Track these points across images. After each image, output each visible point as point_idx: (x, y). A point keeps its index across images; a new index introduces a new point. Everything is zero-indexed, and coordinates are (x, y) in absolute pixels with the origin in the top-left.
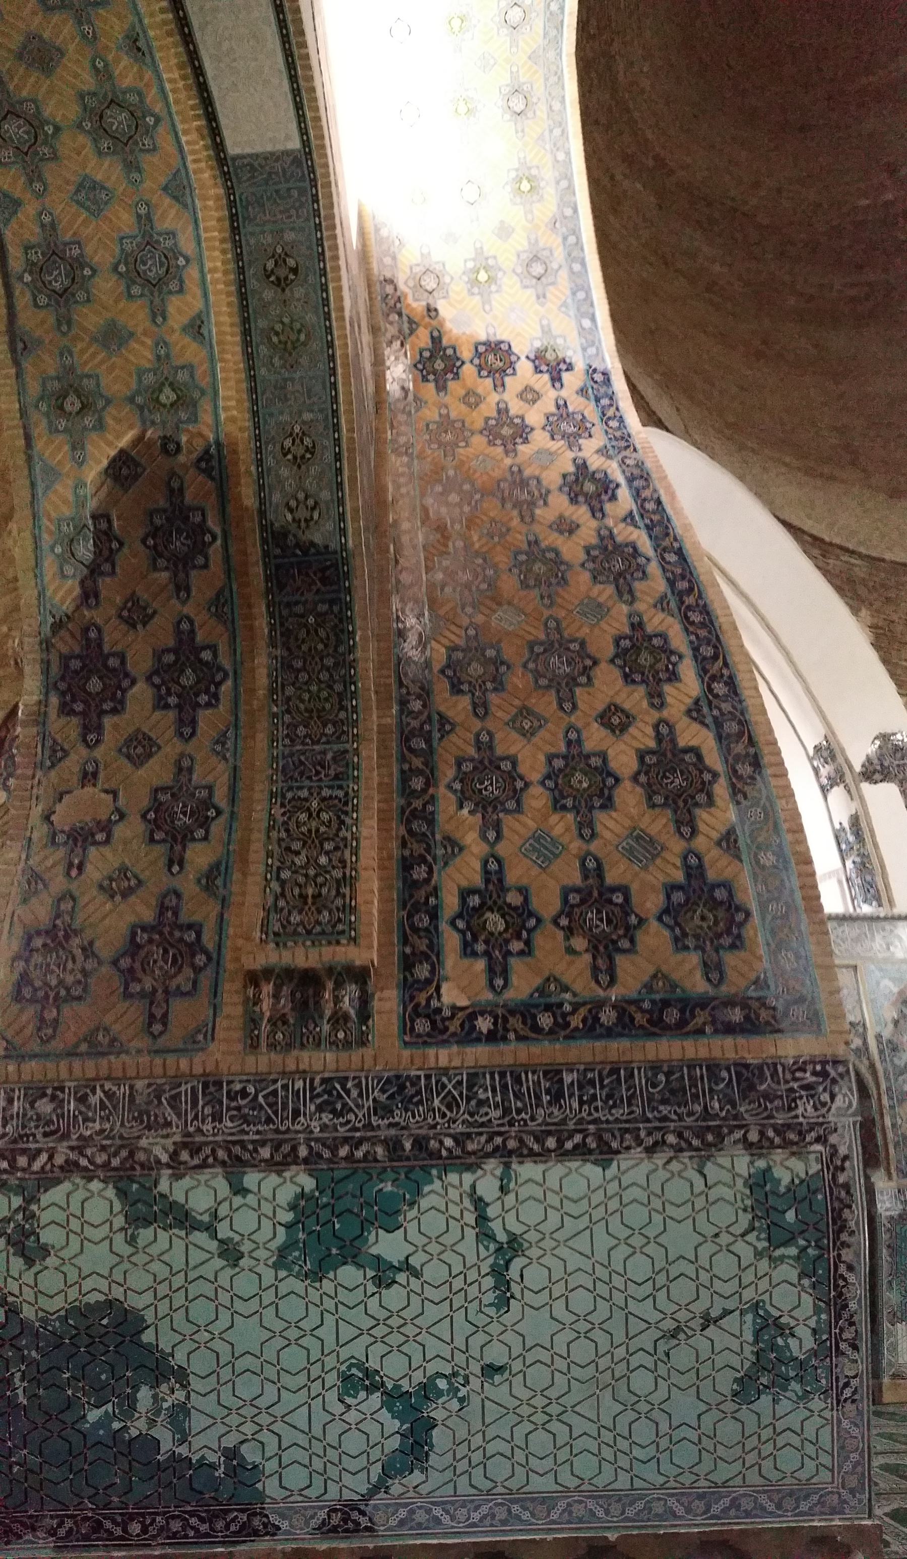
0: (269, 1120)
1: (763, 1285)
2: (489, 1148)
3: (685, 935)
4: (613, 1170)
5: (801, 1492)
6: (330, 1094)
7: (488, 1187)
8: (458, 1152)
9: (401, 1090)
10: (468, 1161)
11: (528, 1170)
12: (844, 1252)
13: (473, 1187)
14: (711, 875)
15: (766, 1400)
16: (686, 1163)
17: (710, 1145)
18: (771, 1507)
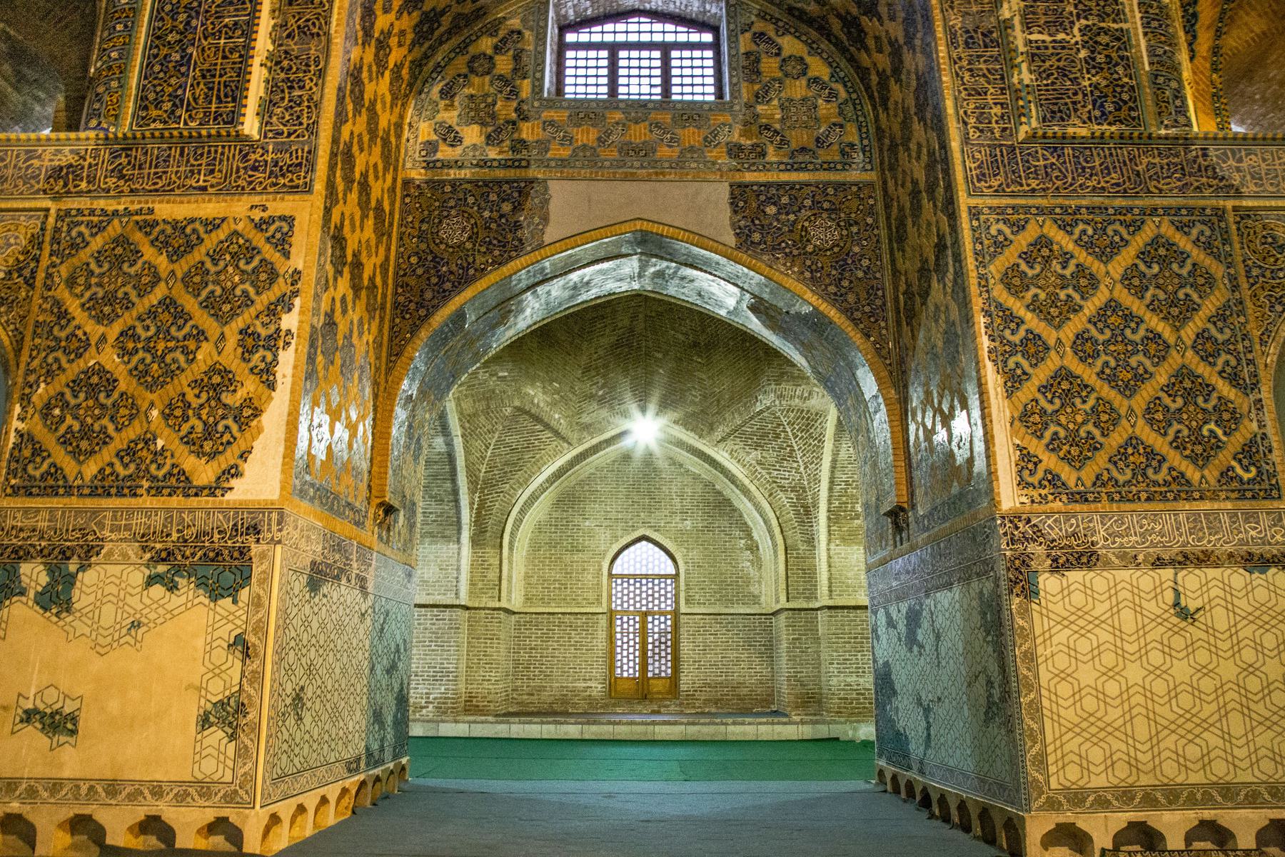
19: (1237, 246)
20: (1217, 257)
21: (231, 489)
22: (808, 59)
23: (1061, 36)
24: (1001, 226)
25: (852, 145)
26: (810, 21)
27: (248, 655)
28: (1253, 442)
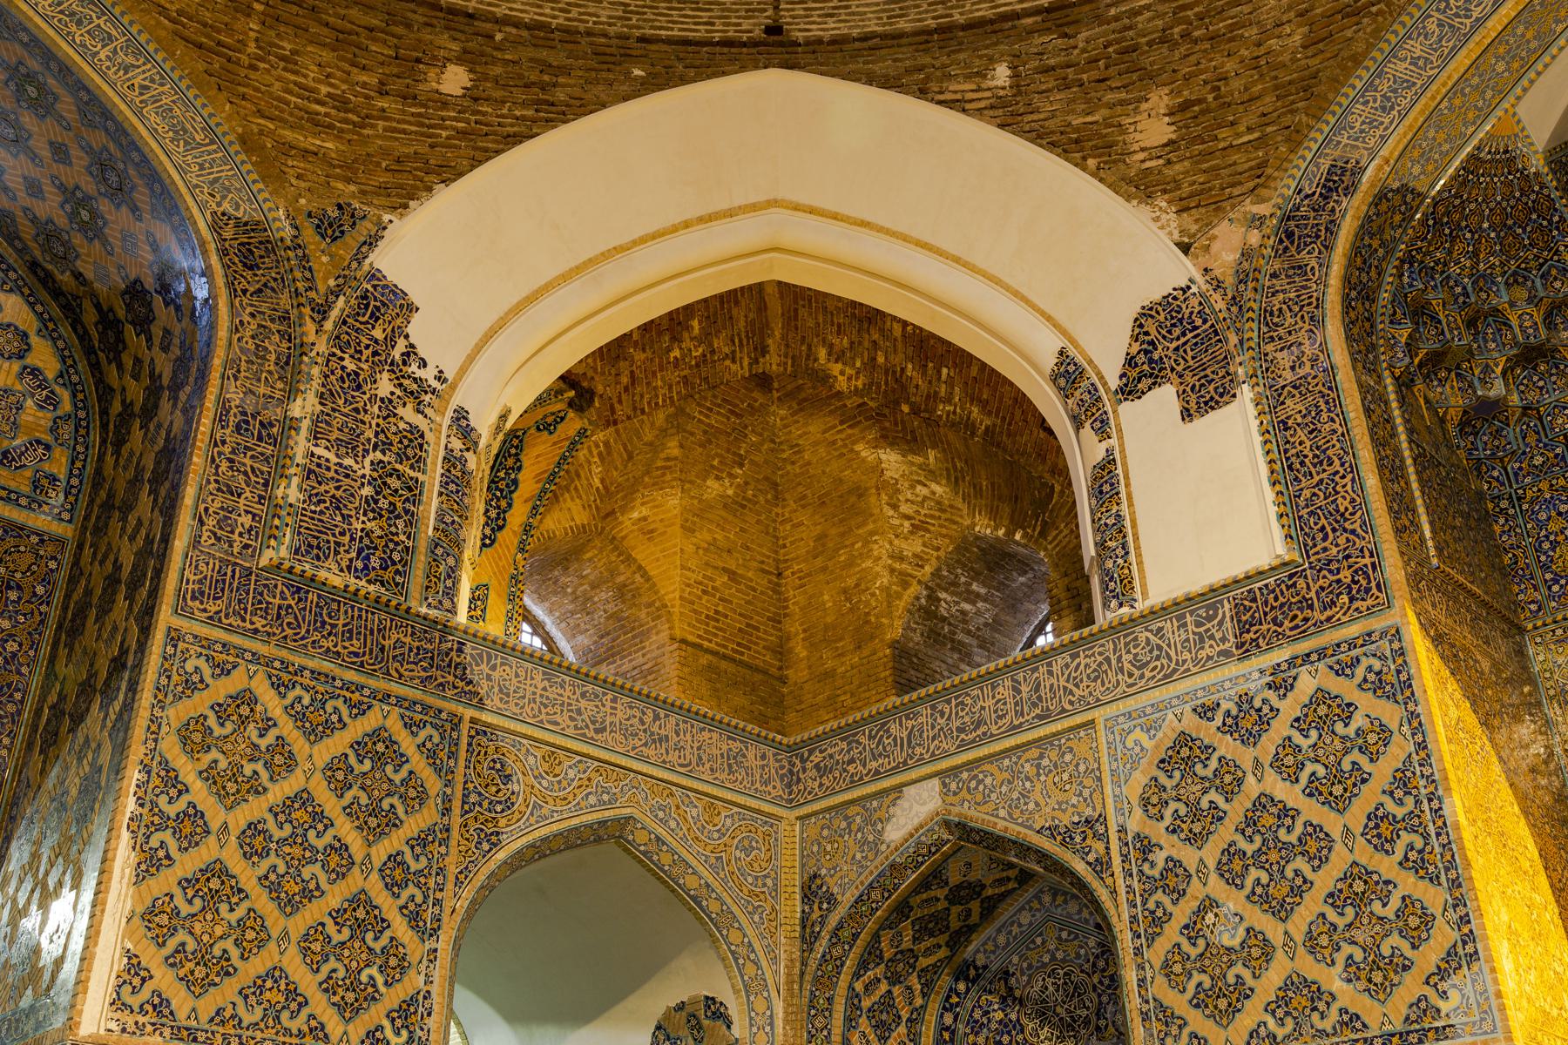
19: (462, 763)
20: (438, 771)
22: (34, 339)
23: (349, 462)
24: (202, 663)
25: (53, 479)
26: (57, 293)
28: (413, 1000)
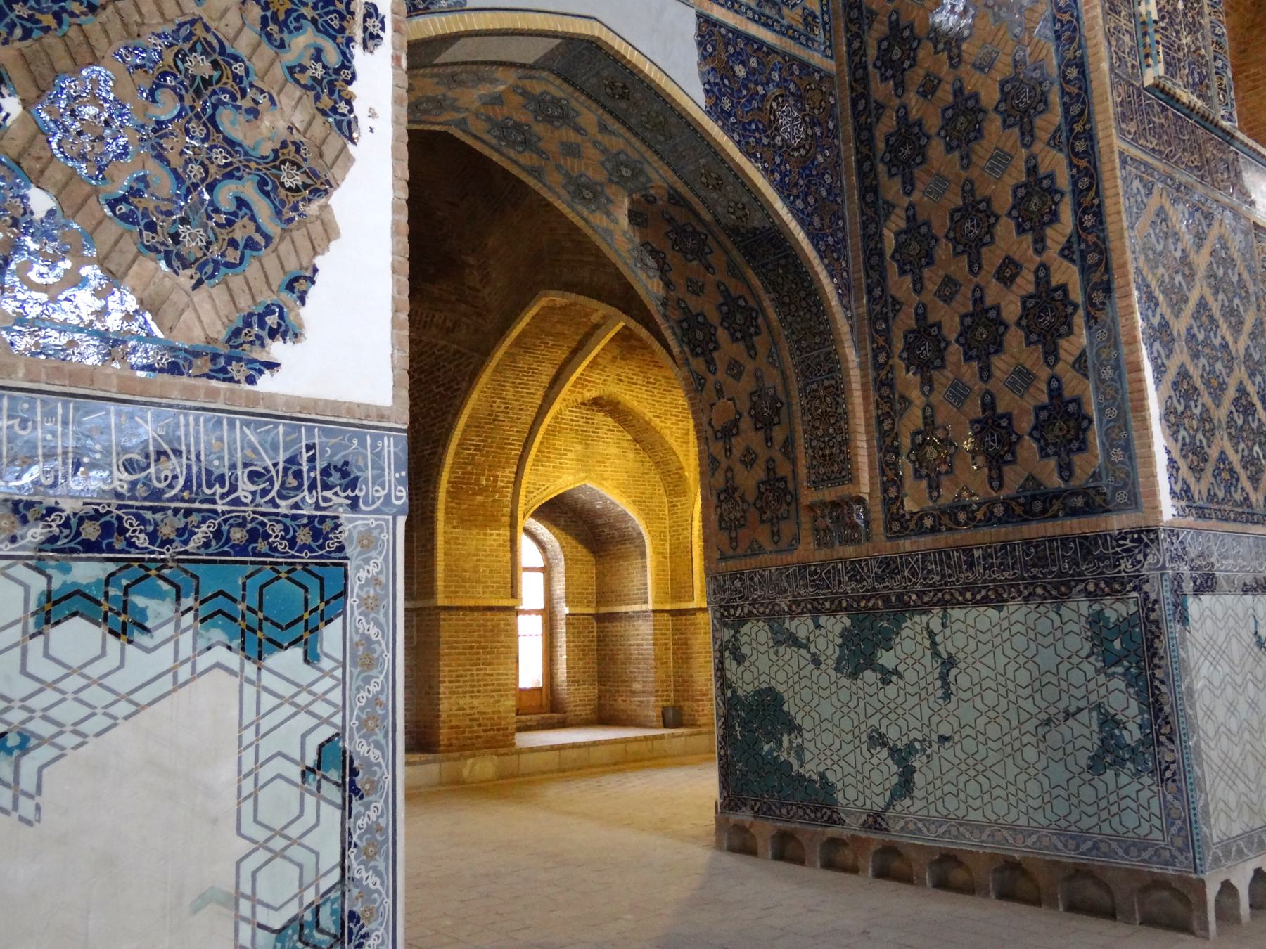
0: (828, 587)
1: (1103, 691)
2: (935, 599)
3: (1047, 445)
4: (1004, 613)
5: (1142, 844)
6: (854, 570)
7: (936, 625)
8: (919, 603)
9: (889, 566)
10: (925, 609)
11: (956, 613)
12: (1157, 672)
13: (928, 624)
14: (1067, 394)
15: (1110, 774)
16: (1048, 605)
17: (1063, 594)
18: (1121, 852)
21: (272, 366)
27: (355, 791)
